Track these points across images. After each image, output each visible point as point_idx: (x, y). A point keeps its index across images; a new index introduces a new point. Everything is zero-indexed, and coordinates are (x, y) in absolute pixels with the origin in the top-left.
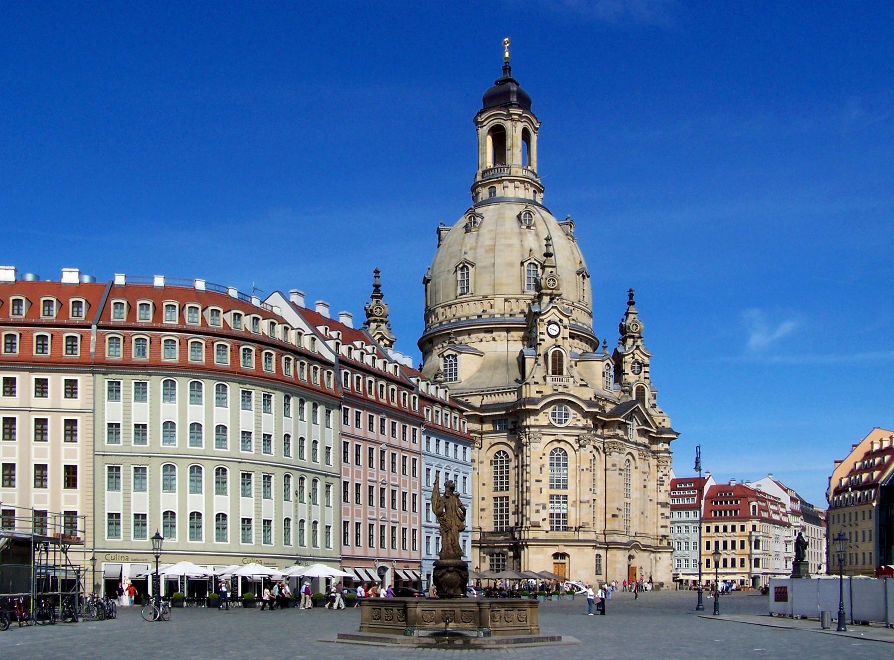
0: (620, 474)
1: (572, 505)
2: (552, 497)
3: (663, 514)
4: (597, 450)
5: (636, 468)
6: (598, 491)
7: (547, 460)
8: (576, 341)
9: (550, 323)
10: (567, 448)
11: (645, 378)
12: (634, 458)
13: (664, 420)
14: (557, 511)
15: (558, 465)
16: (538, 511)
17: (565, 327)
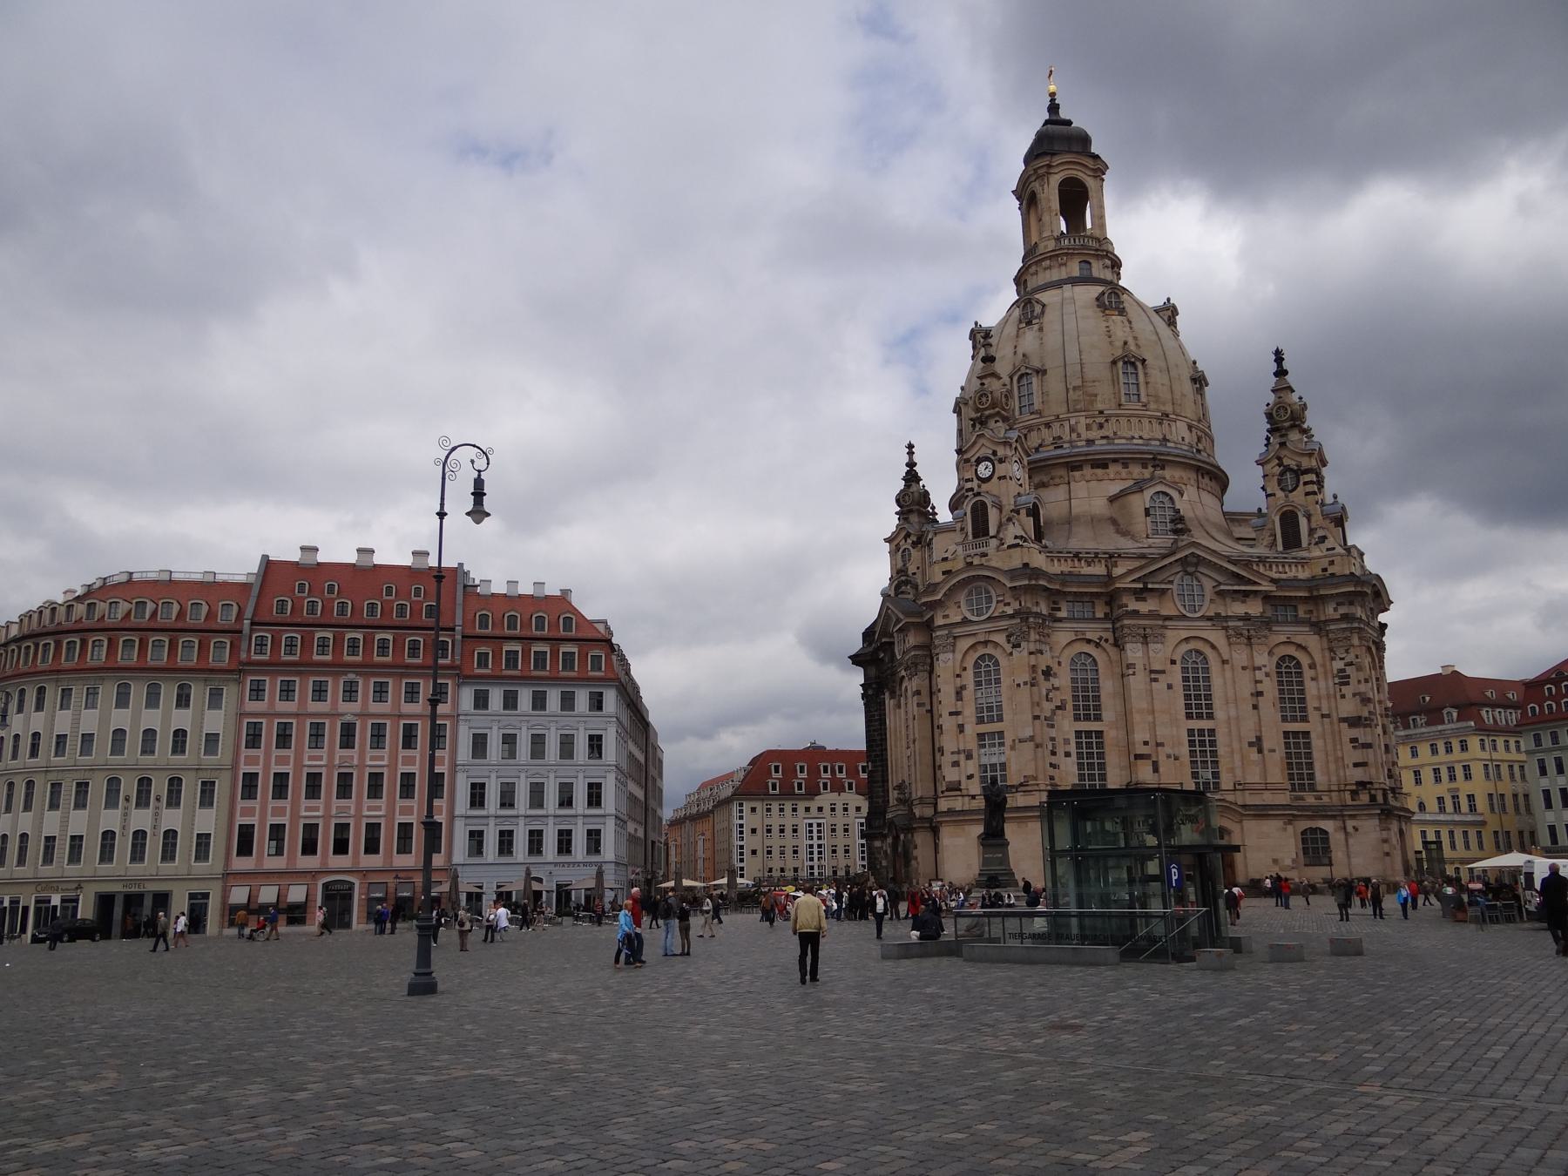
0: (1156, 680)
1: (1013, 748)
2: (981, 736)
3: (1354, 740)
4: (1098, 645)
5: (1224, 662)
6: (1108, 715)
7: (969, 678)
8: (1113, 469)
9: (979, 461)
10: (997, 653)
11: (1307, 494)
12: (1213, 647)
13: (1332, 563)
14: (994, 760)
15: (989, 682)
16: (956, 764)
17: (1001, 461)
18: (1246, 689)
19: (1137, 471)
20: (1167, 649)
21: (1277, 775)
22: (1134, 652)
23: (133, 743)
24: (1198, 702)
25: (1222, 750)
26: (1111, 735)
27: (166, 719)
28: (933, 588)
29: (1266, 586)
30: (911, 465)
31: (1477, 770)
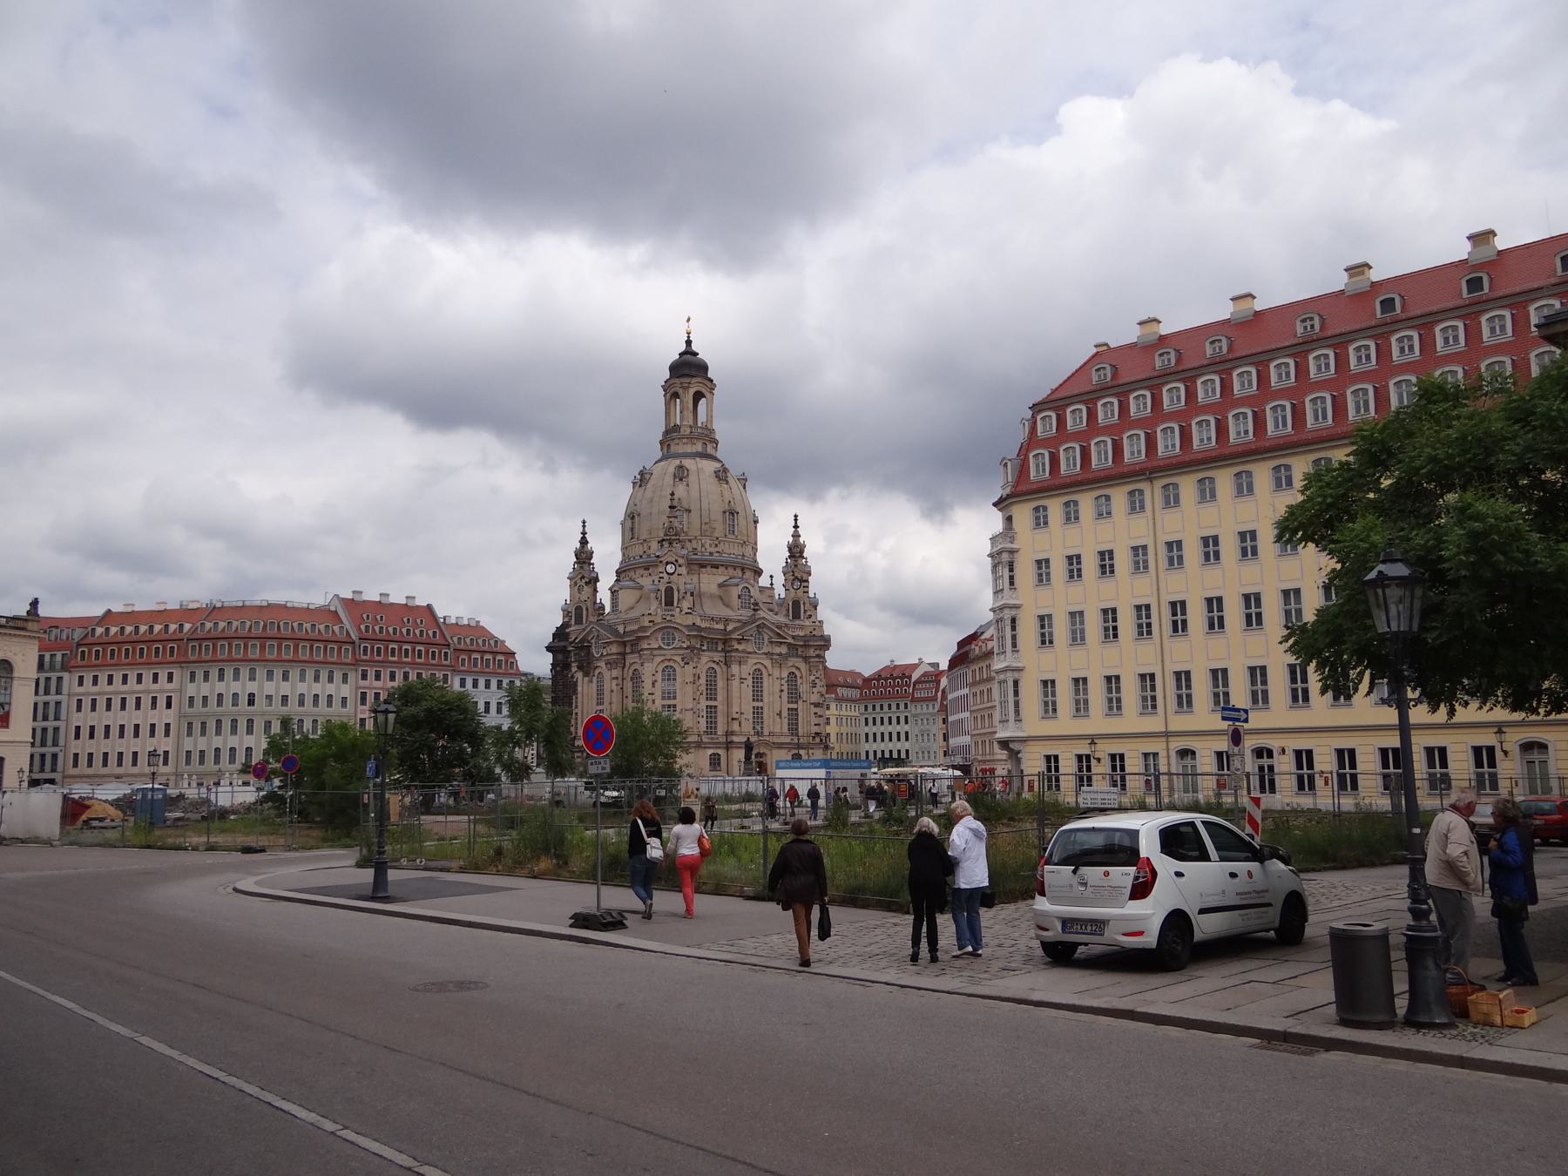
6: (719, 698)
7: (659, 676)
8: (721, 569)
18: (777, 689)
19: (731, 570)
20: (748, 669)
21: (785, 729)
22: (735, 669)
23: (309, 701)
24: (757, 695)
25: (765, 716)
26: (720, 708)
27: (324, 689)
28: (643, 629)
29: (790, 640)
30: (584, 533)
31: (833, 720)
